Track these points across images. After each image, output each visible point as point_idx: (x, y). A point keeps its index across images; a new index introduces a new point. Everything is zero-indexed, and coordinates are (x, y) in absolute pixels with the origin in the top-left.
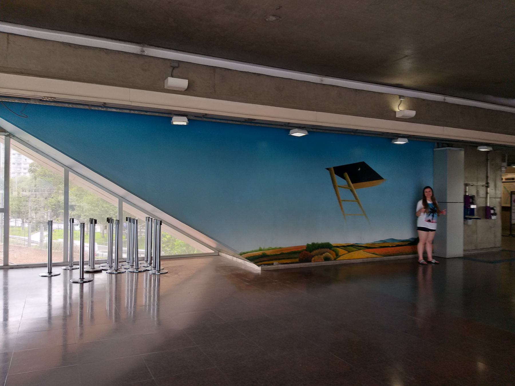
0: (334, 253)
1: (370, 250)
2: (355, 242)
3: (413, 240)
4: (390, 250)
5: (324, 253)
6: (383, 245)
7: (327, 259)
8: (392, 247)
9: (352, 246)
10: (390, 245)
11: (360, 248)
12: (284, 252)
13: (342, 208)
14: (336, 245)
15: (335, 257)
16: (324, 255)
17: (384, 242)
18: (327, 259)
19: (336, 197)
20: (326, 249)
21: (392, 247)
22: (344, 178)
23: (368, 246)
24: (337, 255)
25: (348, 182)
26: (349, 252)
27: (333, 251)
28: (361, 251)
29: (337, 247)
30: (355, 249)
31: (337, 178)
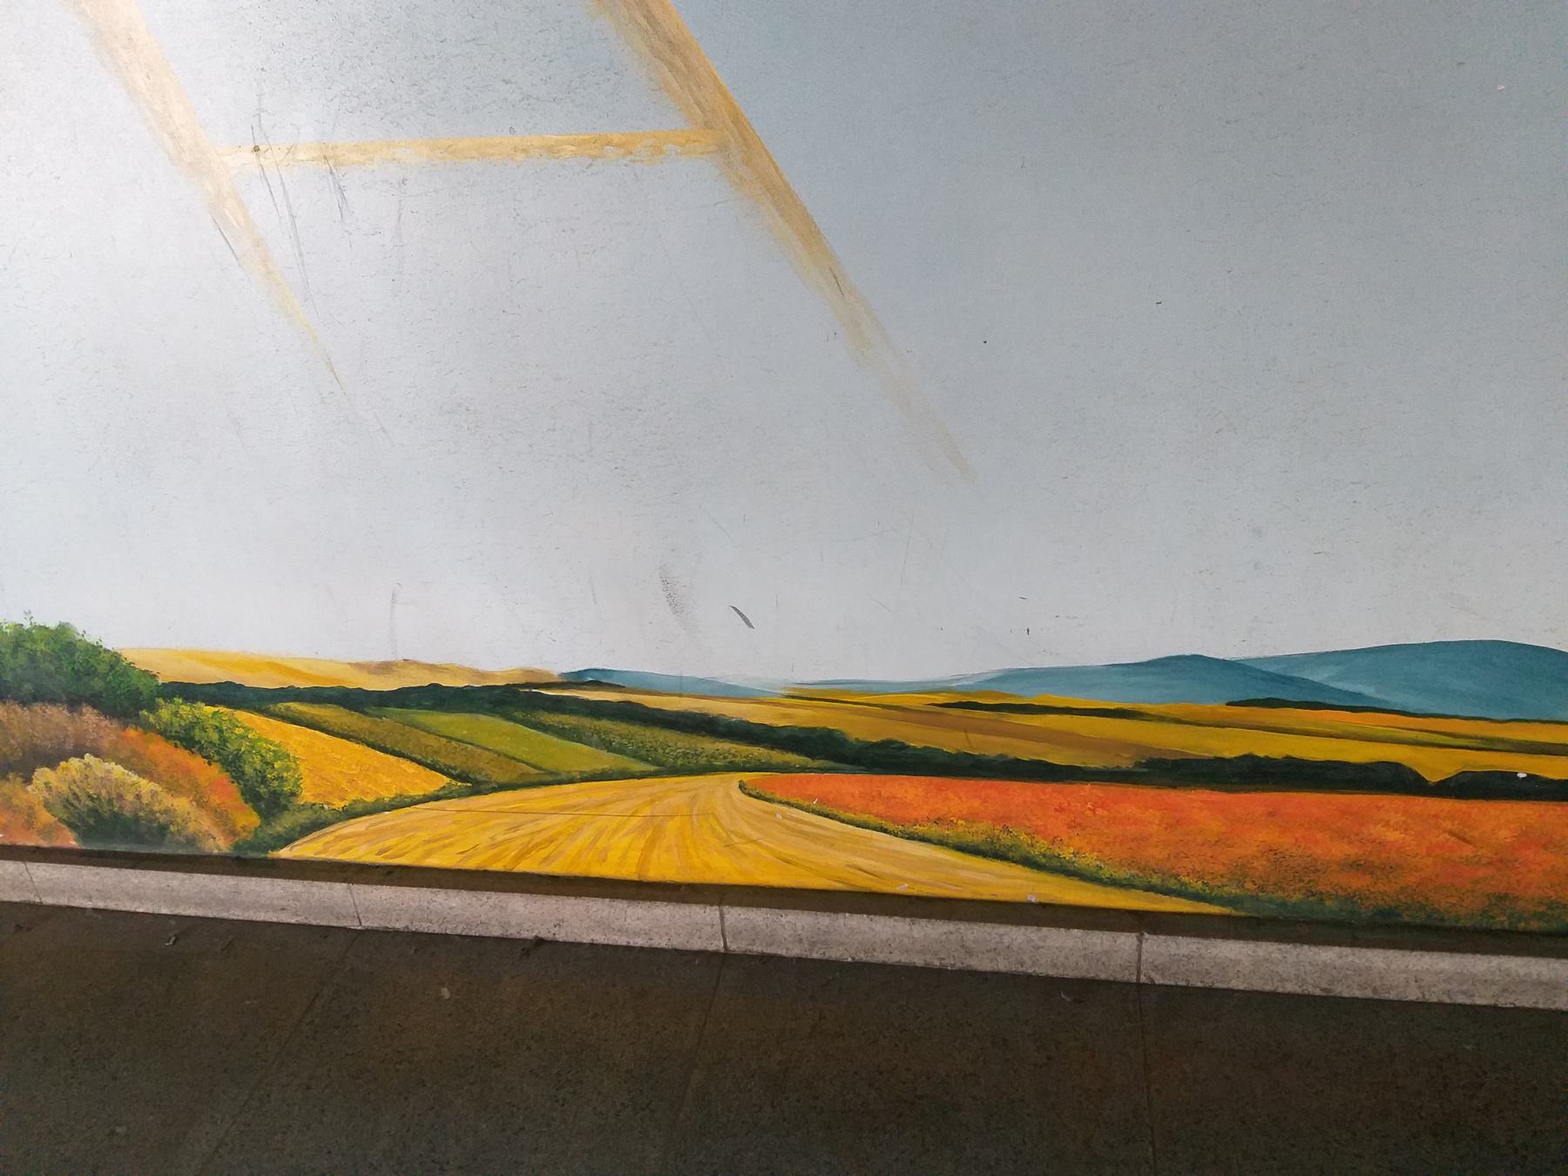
0: (210, 773)
1: (908, 790)
4: (1391, 822)
5: (52, 760)
6: (1237, 740)
7: (113, 836)
9: (516, 700)
10: (1436, 765)
11: (678, 743)
15: (248, 819)
16: (43, 775)
17: (1273, 688)
18: (113, 836)
20: (57, 714)
23: (860, 729)
24: (269, 799)
26: (473, 784)
27: (187, 739)
28: (722, 790)
29: (228, 694)
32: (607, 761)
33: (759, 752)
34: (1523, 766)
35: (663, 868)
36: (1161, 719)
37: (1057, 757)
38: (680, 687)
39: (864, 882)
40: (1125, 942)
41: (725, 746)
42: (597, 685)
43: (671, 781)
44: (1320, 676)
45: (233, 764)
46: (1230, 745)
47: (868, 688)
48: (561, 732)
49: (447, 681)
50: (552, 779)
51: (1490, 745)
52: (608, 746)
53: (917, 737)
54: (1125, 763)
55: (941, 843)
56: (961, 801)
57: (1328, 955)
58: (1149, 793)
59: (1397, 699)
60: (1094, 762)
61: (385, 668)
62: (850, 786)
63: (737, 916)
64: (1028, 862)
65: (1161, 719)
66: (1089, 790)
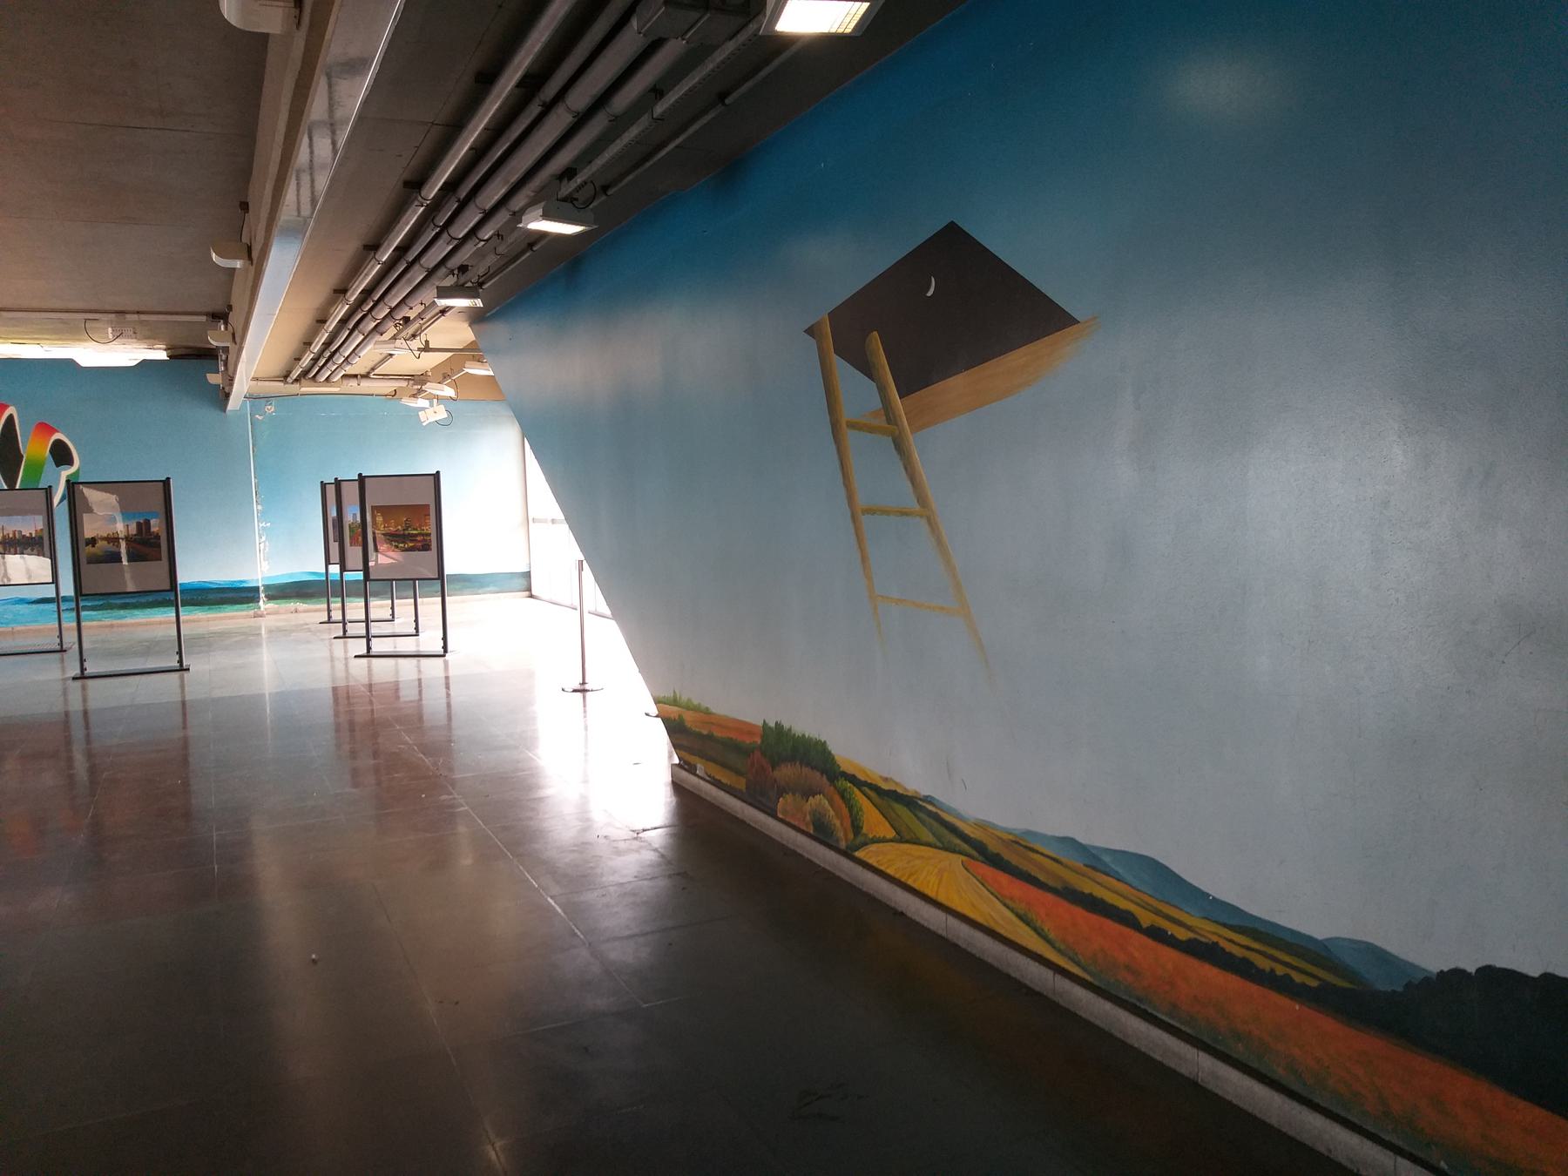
0: (845, 811)
1: (1004, 879)
2: (924, 792)
3: (1382, 983)
8: (1156, 934)
10: (1146, 919)
12: (717, 734)
13: (864, 559)
14: (850, 771)
17: (1094, 859)
18: (821, 832)
19: (842, 492)
21: (1156, 934)
22: (867, 369)
23: (994, 847)
25: (882, 389)
26: (900, 839)
28: (957, 860)
29: (852, 779)
30: (926, 835)
31: (843, 370)
32: (931, 839)
33: (965, 847)
34: (1172, 929)
35: (941, 899)
36: (1066, 866)
37: (1042, 877)
38: (949, 811)
39: (992, 925)
40: (1048, 974)
41: (958, 841)
42: (931, 803)
43: (944, 854)
44: (1107, 859)
45: (850, 808)
46: (1087, 887)
47: (995, 827)
48: (923, 822)
49: (900, 791)
50: (916, 842)
51: (1158, 913)
52: (931, 830)
53: (1007, 855)
54: (1059, 886)
55: (1012, 910)
56: (1017, 889)
57: (1108, 1006)
58: (1067, 905)
59: (1129, 878)
60: (1051, 883)
61: (886, 780)
62: (989, 871)
63: (952, 921)
64: (1035, 930)
65: (1066, 866)
66: (1050, 897)
